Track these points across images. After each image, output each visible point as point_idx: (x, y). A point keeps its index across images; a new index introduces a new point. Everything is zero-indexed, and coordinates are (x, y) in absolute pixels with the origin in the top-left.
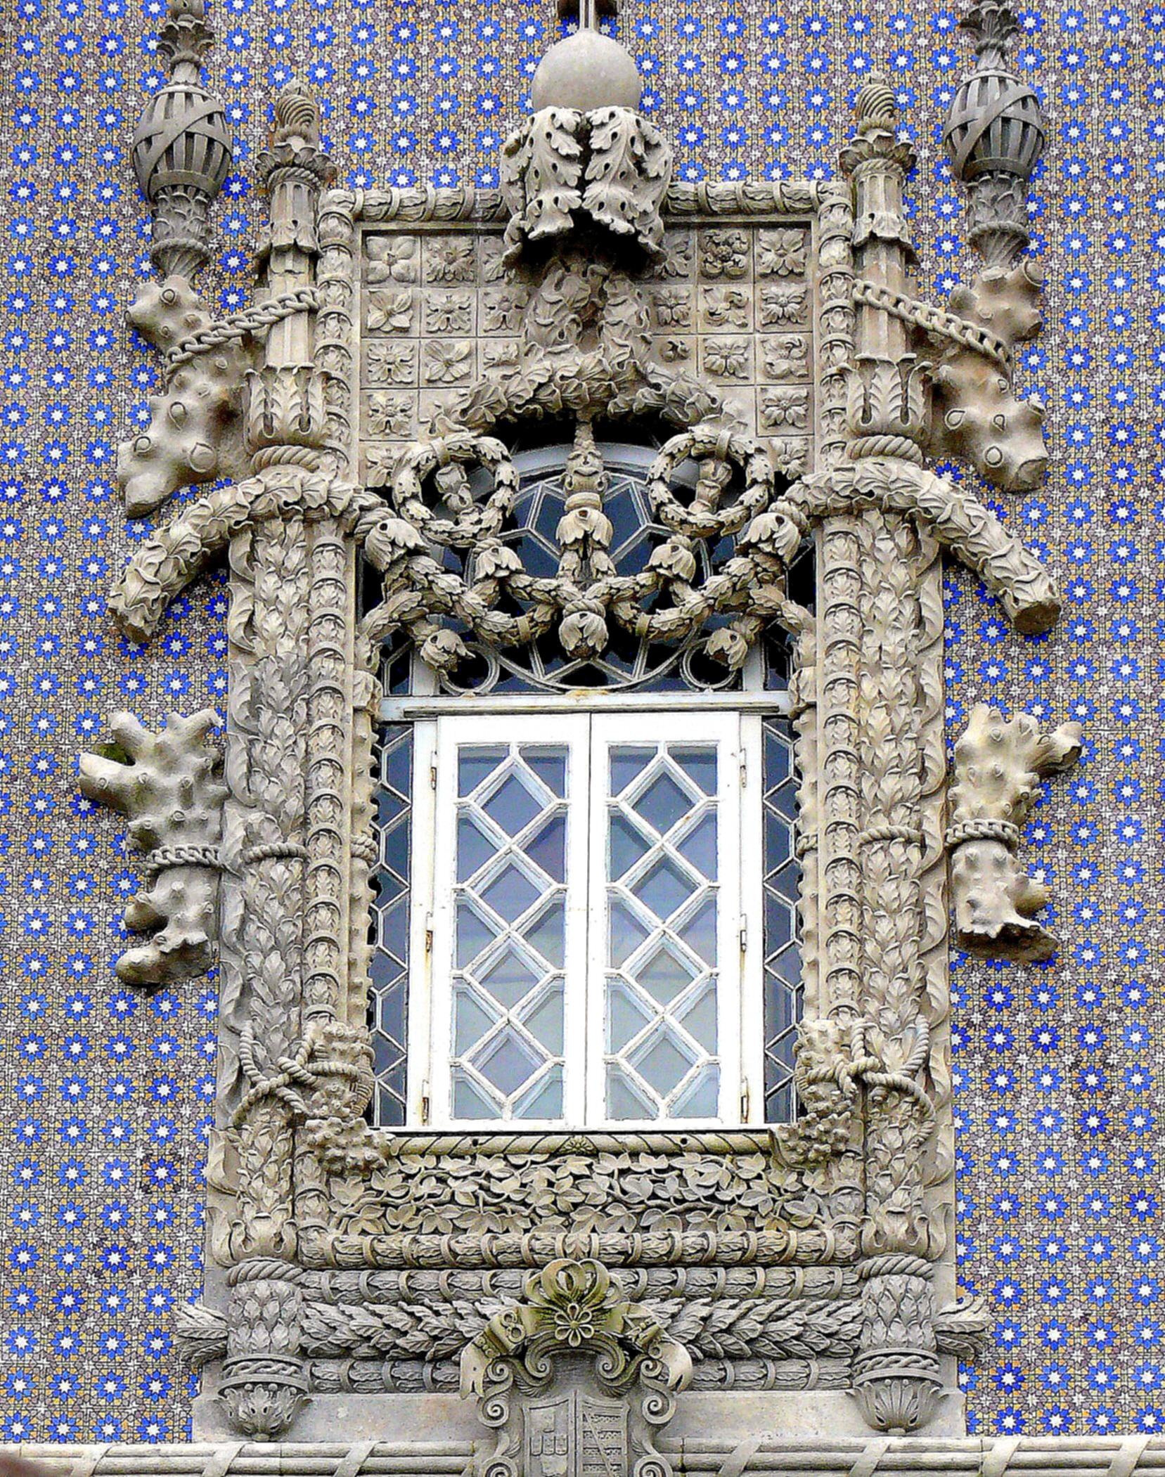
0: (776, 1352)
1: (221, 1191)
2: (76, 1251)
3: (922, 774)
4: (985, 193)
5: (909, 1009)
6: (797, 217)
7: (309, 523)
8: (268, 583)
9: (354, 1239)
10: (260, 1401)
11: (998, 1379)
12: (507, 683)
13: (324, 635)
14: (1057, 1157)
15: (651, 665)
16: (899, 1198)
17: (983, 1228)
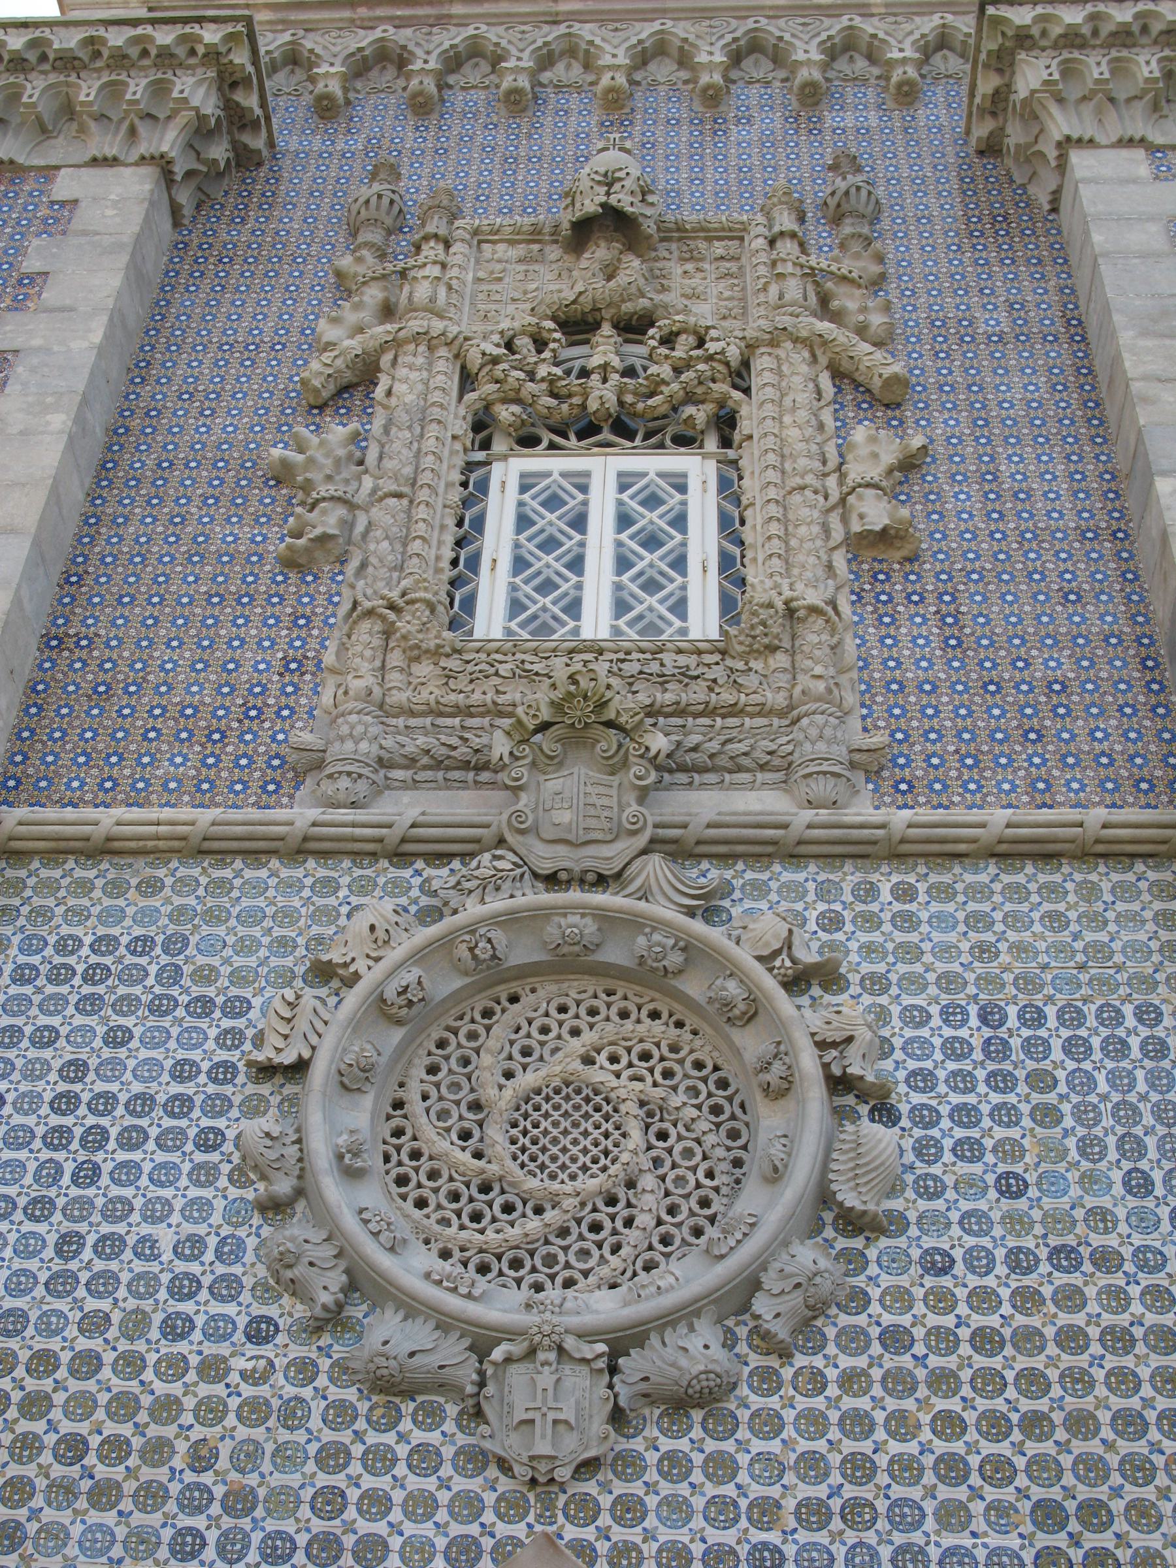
0: (729, 765)
1: (333, 671)
2: (226, 709)
3: (824, 463)
4: (848, 221)
5: (820, 572)
6: (736, 234)
7: (430, 348)
8: (402, 372)
9: (425, 694)
10: (344, 783)
11: (896, 787)
12: (552, 446)
13: (436, 397)
14: (929, 661)
15: (645, 438)
16: (818, 670)
17: (879, 699)
